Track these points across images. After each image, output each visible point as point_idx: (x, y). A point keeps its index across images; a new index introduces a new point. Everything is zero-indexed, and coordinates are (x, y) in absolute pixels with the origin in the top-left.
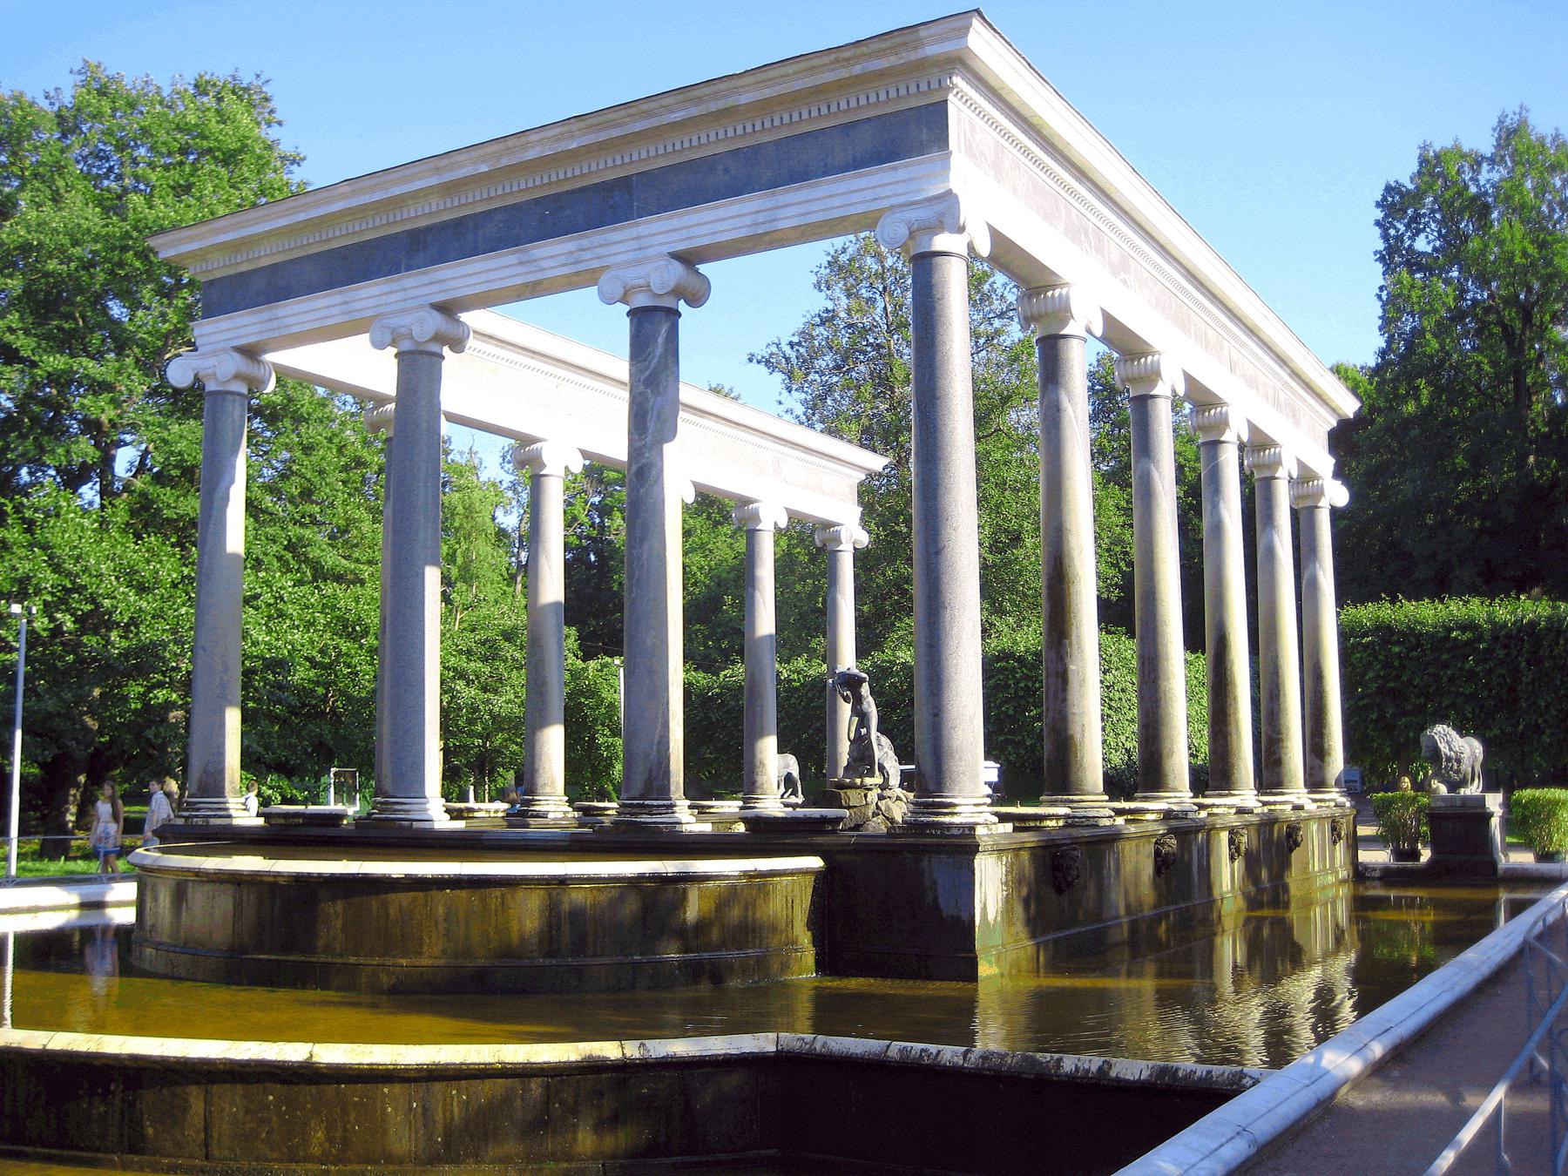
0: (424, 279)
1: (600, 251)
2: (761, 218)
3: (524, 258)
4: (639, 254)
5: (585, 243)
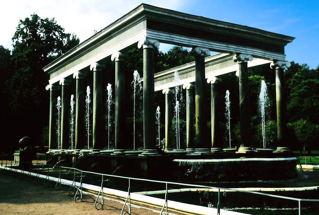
0: (208, 42)
1: (240, 50)
2: (264, 54)
3: (227, 46)
4: (245, 53)
5: (238, 48)
